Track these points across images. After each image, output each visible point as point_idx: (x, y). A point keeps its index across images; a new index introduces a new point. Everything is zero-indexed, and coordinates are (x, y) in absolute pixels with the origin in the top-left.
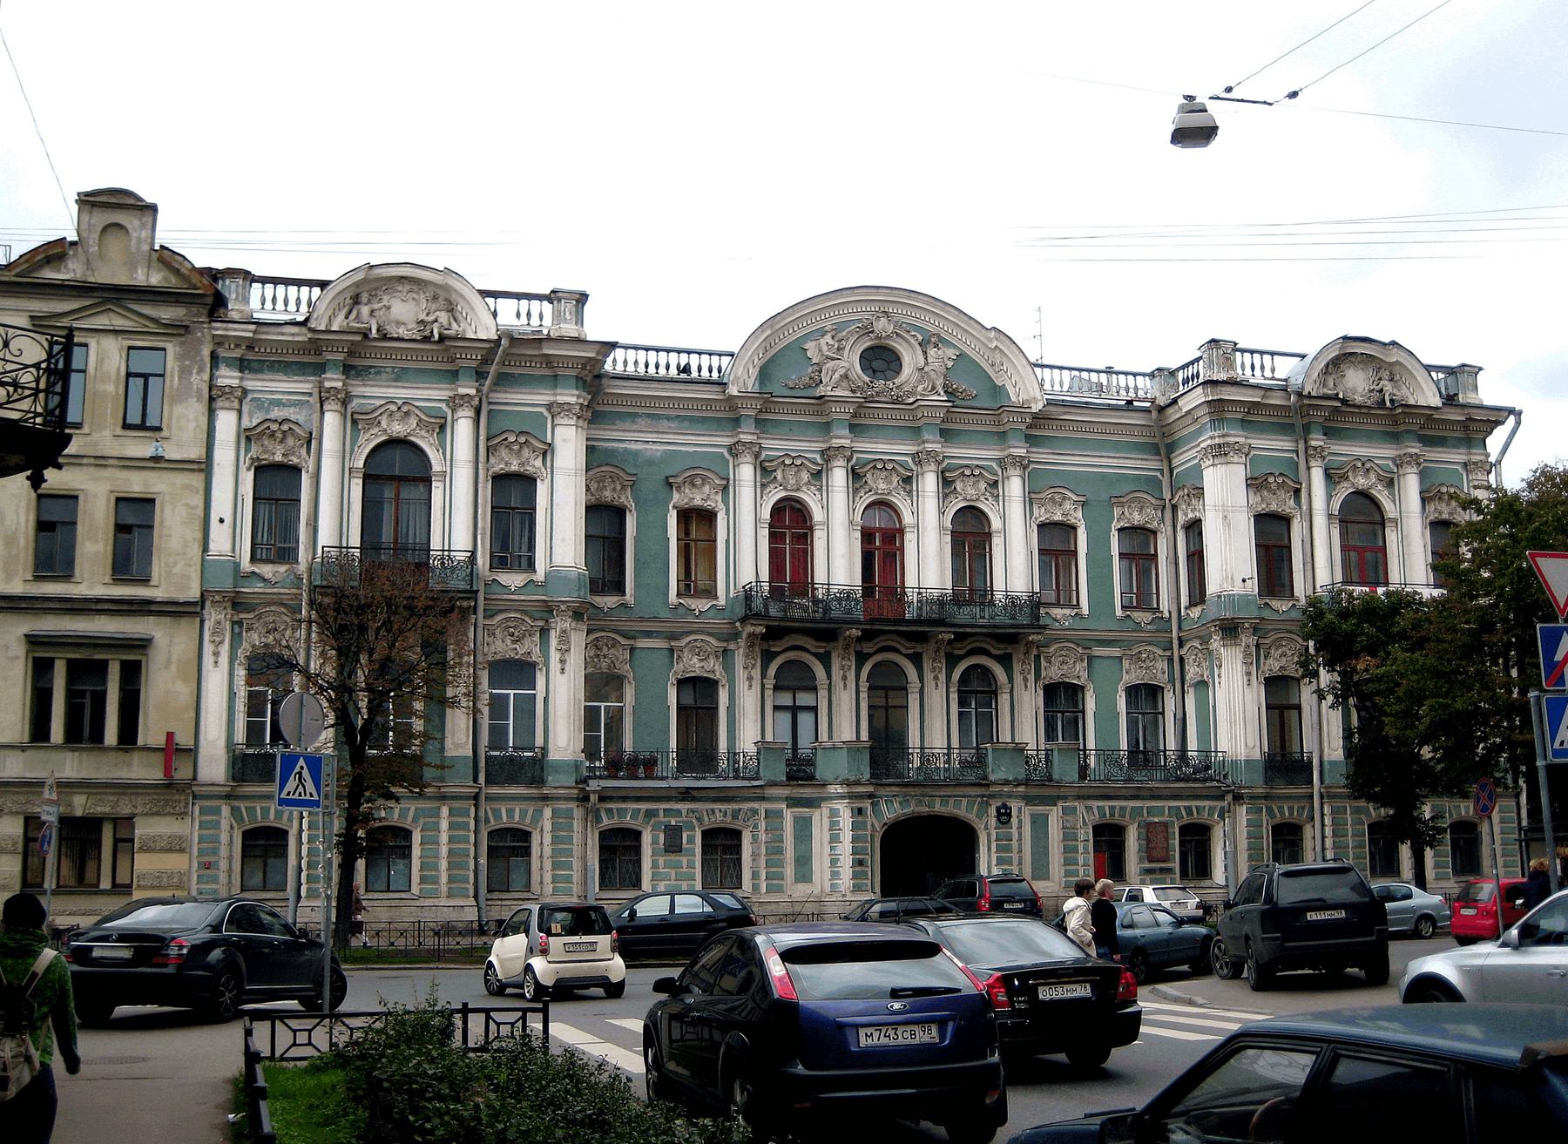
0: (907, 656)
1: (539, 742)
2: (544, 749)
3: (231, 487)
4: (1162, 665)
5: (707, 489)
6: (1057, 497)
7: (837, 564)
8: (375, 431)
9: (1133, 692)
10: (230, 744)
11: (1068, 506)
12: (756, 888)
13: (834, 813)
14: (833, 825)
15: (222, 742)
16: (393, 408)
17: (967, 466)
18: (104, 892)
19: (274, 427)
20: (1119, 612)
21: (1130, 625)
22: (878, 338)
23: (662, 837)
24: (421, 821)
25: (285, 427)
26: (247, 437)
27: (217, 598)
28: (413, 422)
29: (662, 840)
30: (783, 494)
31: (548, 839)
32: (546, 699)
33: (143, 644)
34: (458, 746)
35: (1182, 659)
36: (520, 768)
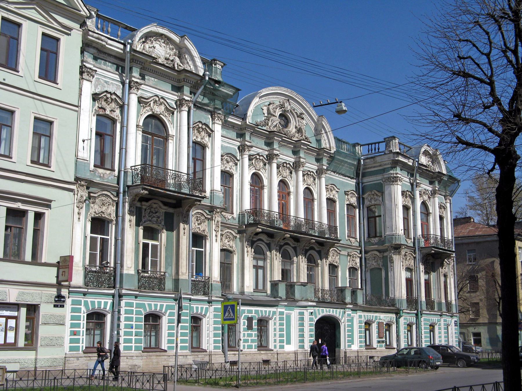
0: (292, 247)
1: (207, 274)
2: (209, 278)
3: (88, 124)
4: (358, 260)
5: (231, 164)
6: (332, 189)
7: (271, 203)
8: (148, 108)
9: (350, 269)
10: (84, 265)
11: (334, 192)
12: (275, 347)
13: (301, 314)
14: (302, 319)
15: (81, 264)
16: (157, 99)
17: (309, 171)
18: (21, 349)
19: (109, 95)
20: (347, 238)
21: (349, 243)
22: (285, 111)
23: (246, 321)
24: (169, 311)
25: (114, 97)
26: (95, 97)
27: (83, 183)
28: (163, 107)
29: (246, 325)
30: (254, 171)
31: (211, 322)
32: (210, 253)
33: (47, 204)
34: (183, 274)
35: (365, 259)
36: (202, 287)
